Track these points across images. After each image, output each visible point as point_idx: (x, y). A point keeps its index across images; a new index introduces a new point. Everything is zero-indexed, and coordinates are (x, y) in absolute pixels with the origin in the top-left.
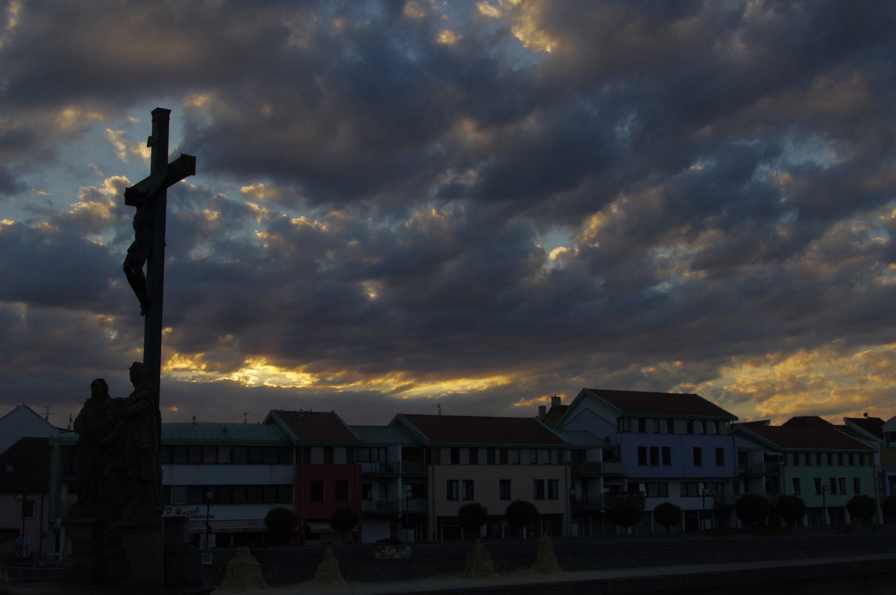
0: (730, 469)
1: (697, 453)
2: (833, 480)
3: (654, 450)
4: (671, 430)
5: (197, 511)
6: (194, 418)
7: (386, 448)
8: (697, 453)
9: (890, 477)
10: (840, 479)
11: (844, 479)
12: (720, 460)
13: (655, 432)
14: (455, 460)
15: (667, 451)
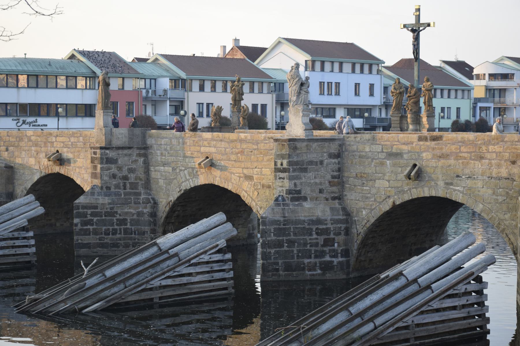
0: (377, 99)
1: (357, 86)
2: (443, 109)
3: (329, 84)
4: (341, 70)
5: (36, 121)
6: (25, 54)
7: (155, 79)
8: (357, 86)
9: (480, 107)
10: (448, 108)
11: (450, 108)
12: (372, 94)
13: (330, 72)
14: (202, 88)
15: (338, 84)
